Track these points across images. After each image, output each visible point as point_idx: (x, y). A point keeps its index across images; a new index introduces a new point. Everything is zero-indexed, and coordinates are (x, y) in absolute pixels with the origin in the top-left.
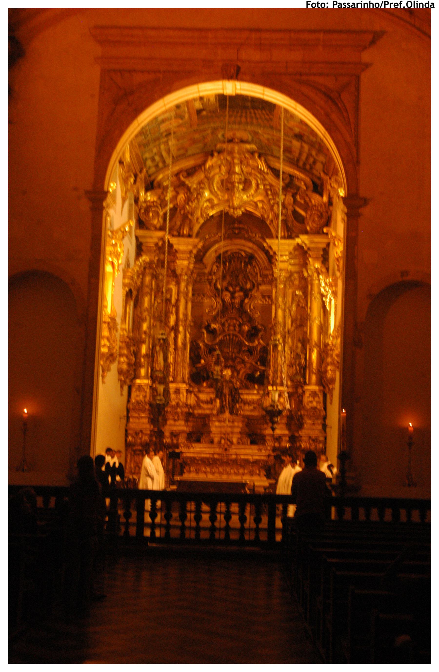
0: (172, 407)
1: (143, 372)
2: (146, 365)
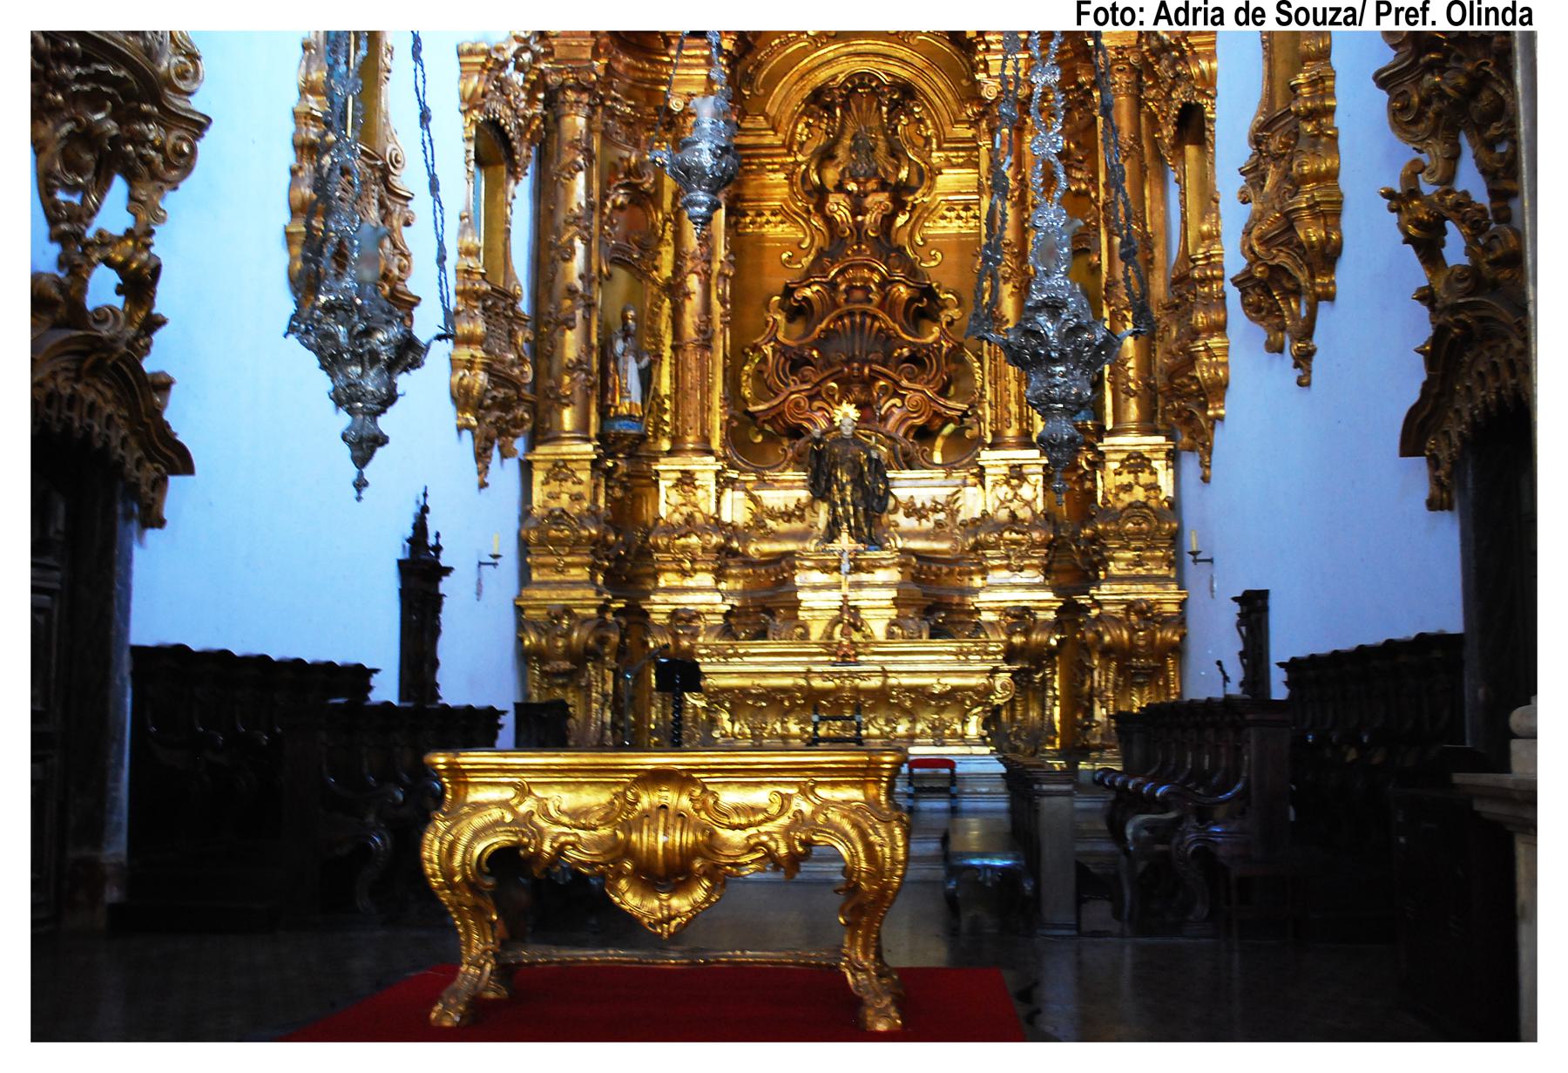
0: (671, 530)
1: (568, 418)
2: (578, 398)
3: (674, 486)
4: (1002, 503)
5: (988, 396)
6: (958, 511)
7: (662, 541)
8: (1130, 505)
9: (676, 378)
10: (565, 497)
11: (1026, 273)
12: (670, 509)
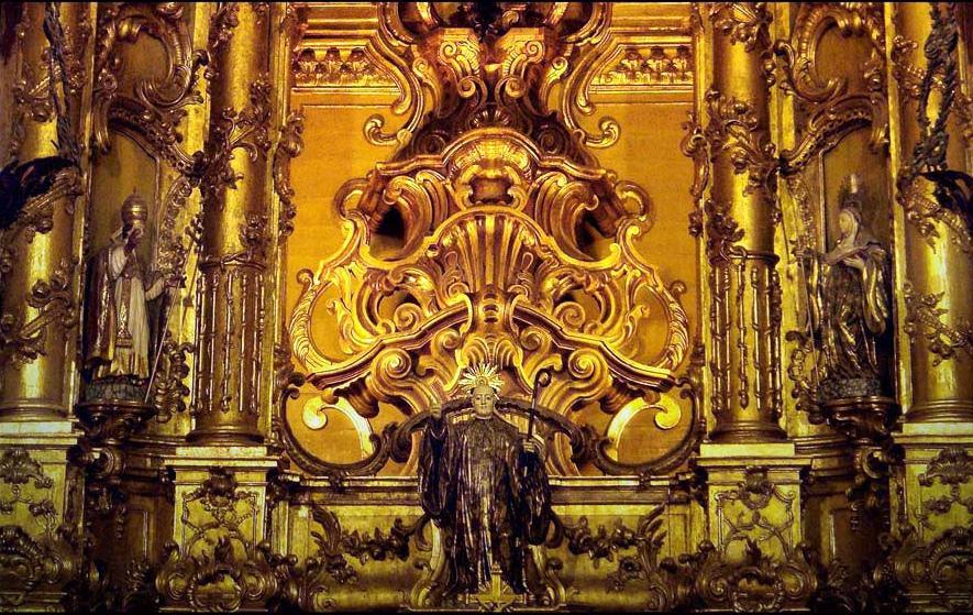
0: (191, 566)
1: (33, 376)
3: (199, 495)
4: (735, 530)
5: (709, 355)
6: (659, 543)
7: (177, 584)
8: (947, 534)
9: (207, 316)
10: (22, 508)
11: (768, 156)
12: (190, 533)
